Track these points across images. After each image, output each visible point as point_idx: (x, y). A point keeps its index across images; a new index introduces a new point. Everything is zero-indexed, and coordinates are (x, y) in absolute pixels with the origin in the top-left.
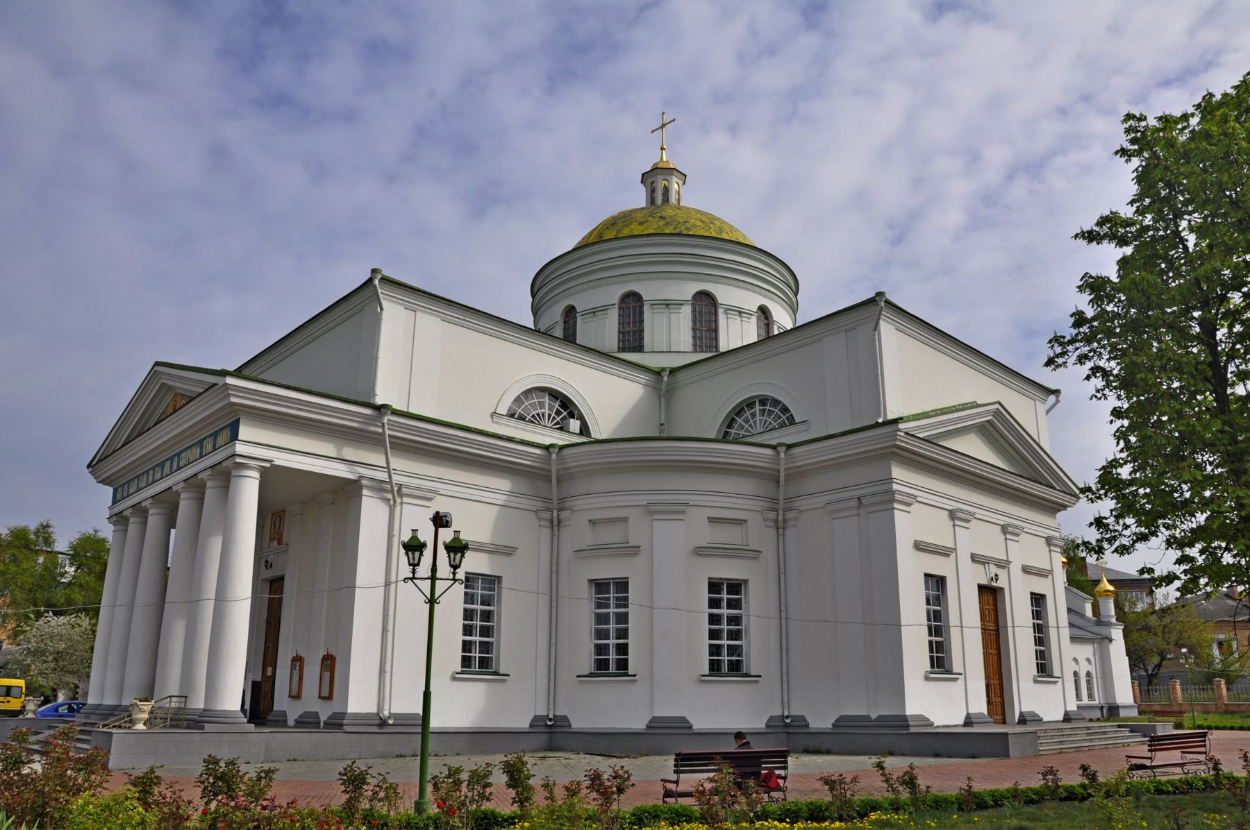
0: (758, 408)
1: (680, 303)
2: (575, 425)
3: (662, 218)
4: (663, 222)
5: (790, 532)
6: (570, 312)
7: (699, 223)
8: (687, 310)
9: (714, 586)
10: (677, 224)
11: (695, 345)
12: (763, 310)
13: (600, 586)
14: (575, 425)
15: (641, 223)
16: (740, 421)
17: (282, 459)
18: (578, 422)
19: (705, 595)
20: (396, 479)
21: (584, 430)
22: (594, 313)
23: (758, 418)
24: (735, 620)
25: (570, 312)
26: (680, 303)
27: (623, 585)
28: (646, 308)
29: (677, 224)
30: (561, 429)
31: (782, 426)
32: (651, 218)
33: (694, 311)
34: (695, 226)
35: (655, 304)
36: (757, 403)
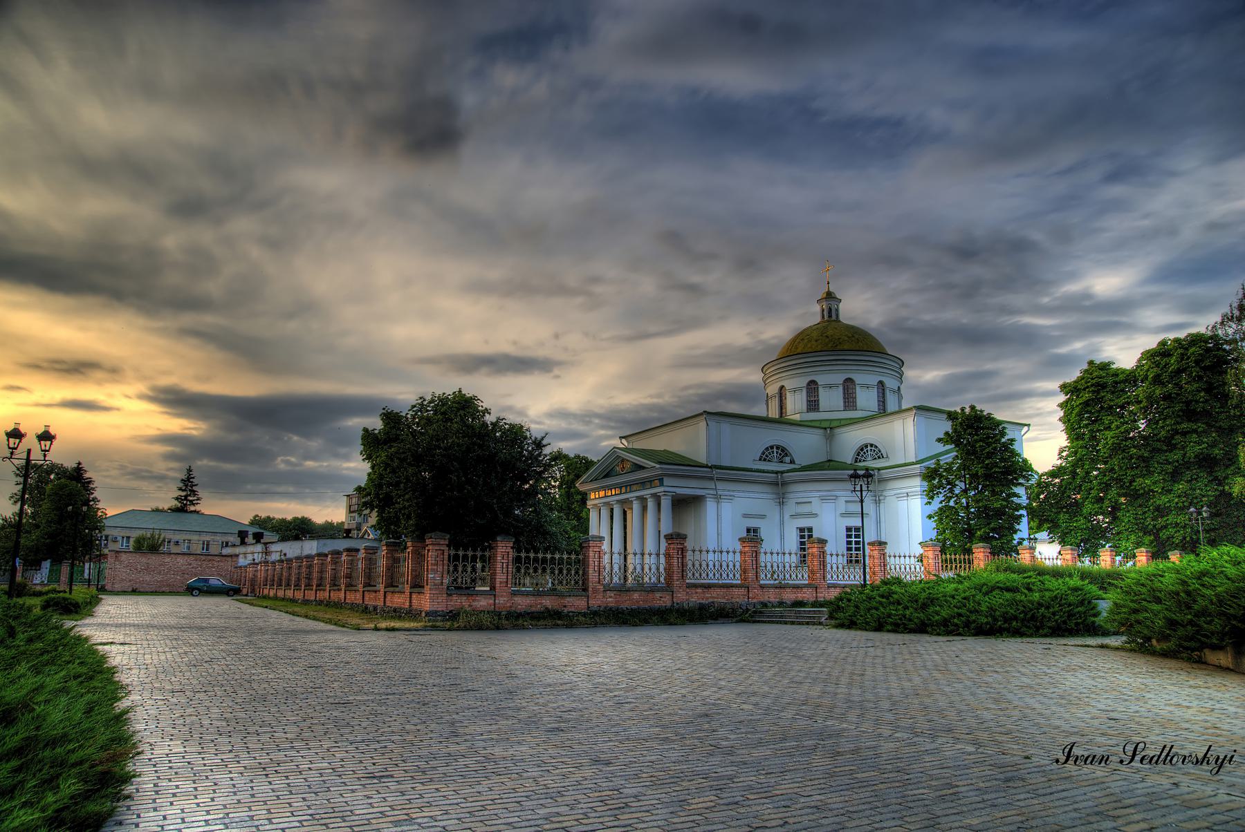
0: (869, 448)
1: (837, 386)
3: (827, 337)
5: (882, 505)
7: (846, 338)
8: (841, 388)
9: (849, 529)
11: (845, 406)
12: (881, 383)
13: (802, 530)
14: (787, 459)
17: (679, 491)
19: (844, 533)
20: (719, 493)
21: (792, 462)
24: (857, 543)
26: (837, 386)
27: (810, 530)
28: (821, 390)
30: (782, 462)
31: (879, 458)
33: (844, 389)
35: (825, 386)
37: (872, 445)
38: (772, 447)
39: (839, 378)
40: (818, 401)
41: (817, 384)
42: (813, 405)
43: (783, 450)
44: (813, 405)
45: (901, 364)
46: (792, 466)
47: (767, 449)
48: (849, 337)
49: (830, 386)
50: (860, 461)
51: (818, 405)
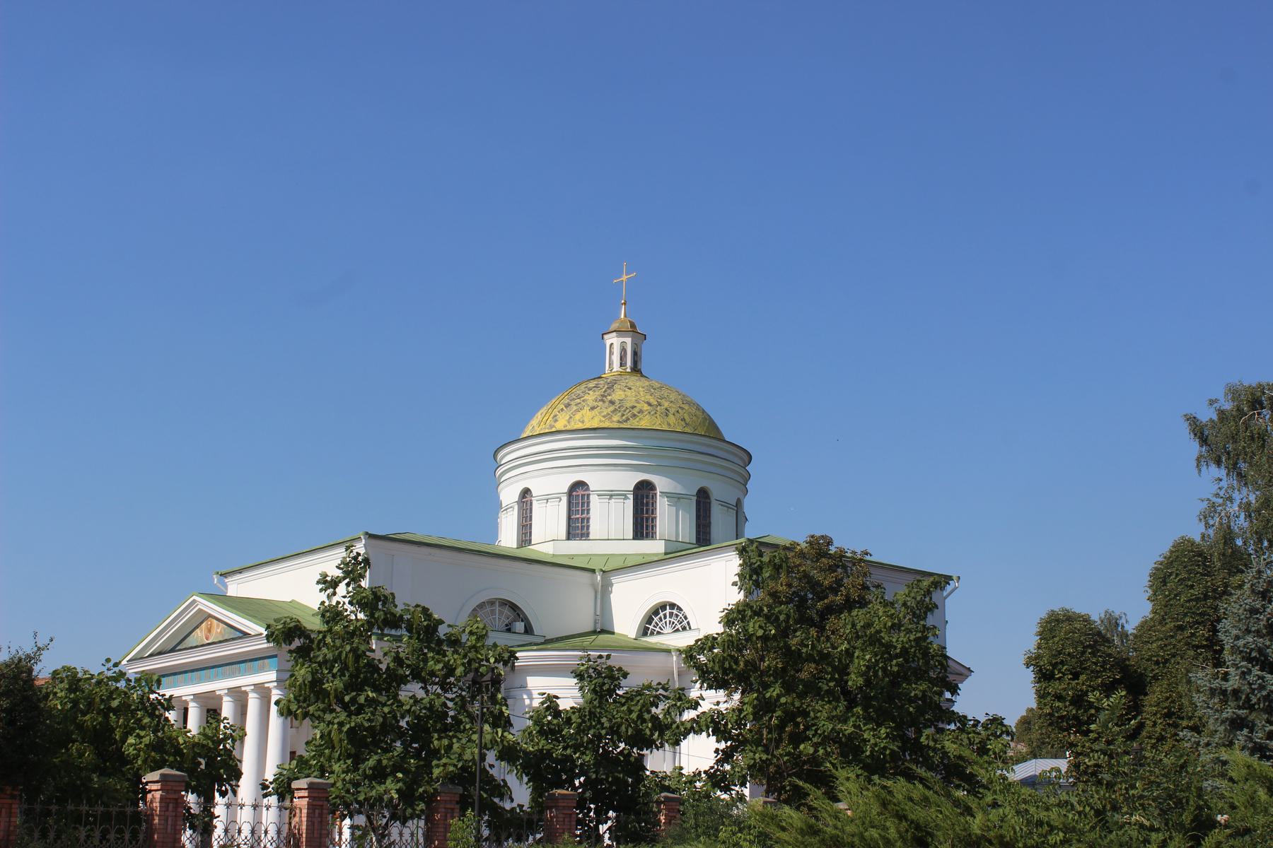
0: (668, 611)
2: (520, 626)
3: (612, 402)
4: (612, 408)
6: (526, 492)
7: (646, 407)
10: (625, 411)
15: (593, 408)
16: (656, 619)
18: (523, 624)
21: (528, 630)
22: (547, 500)
23: (668, 619)
25: (526, 492)
28: (594, 501)
29: (625, 411)
30: (509, 630)
31: (684, 629)
32: (601, 403)
34: (641, 411)
36: (668, 607)
37: (673, 606)
38: (492, 603)
39: (628, 480)
40: (588, 519)
41: (588, 489)
42: (577, 527)
43: (514, 607)
44: (577, 527)
45: (746, 458)
46: (528, 638)
47: (481, 606)
48: (650, 404)
49: (611, 495)
50: (652, 634)
51: (588, 527)
